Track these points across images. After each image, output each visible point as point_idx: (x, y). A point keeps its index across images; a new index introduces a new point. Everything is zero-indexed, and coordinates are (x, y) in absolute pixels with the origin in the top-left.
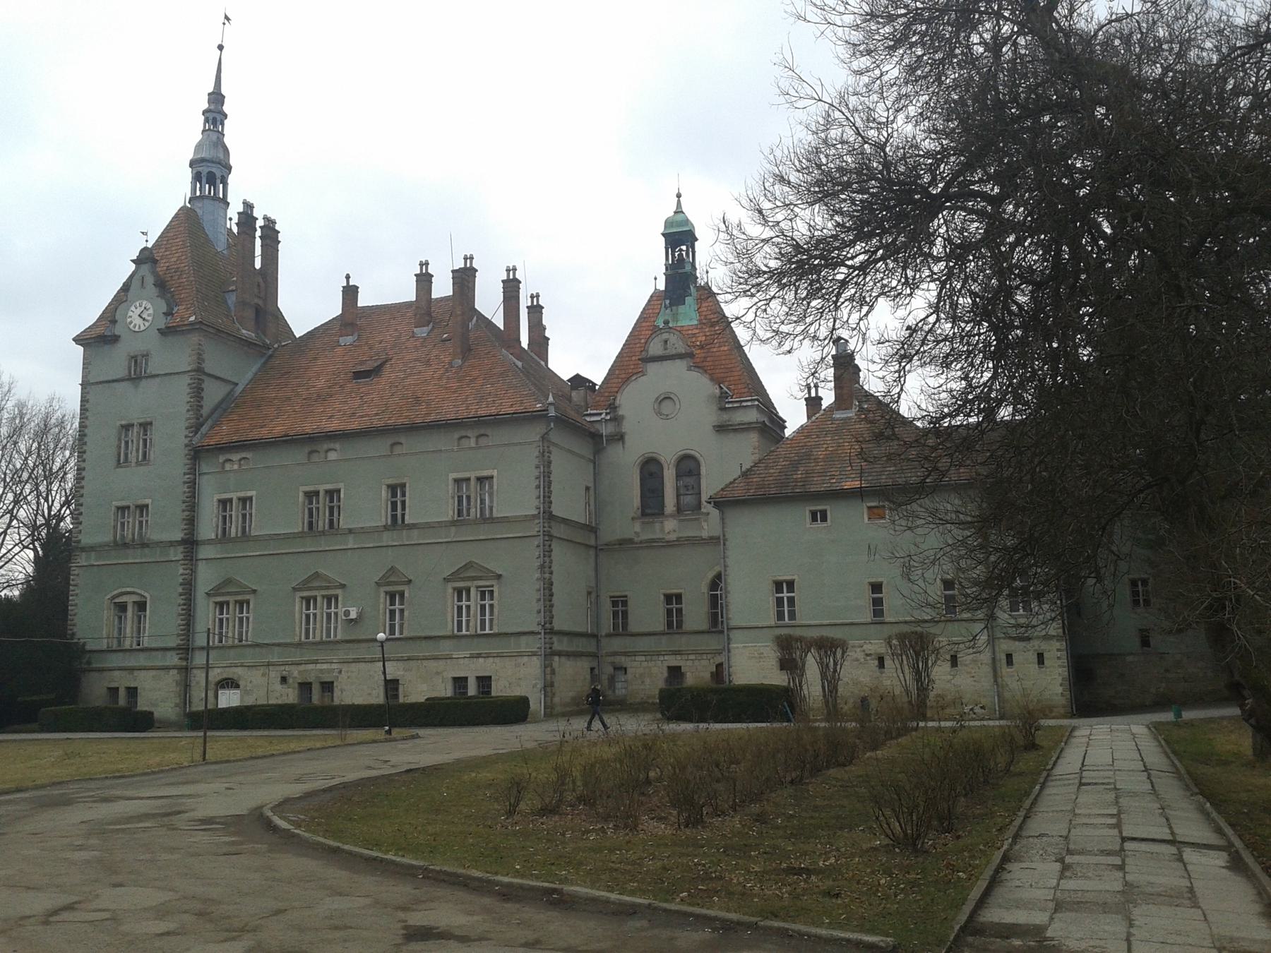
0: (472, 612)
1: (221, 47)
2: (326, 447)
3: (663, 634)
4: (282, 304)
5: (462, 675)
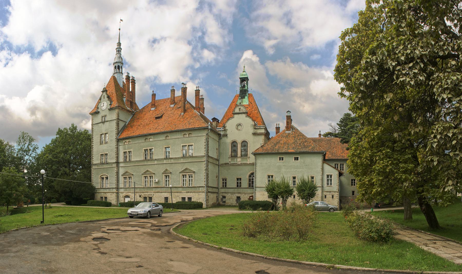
0: (187, 181)
2: (149, 137)
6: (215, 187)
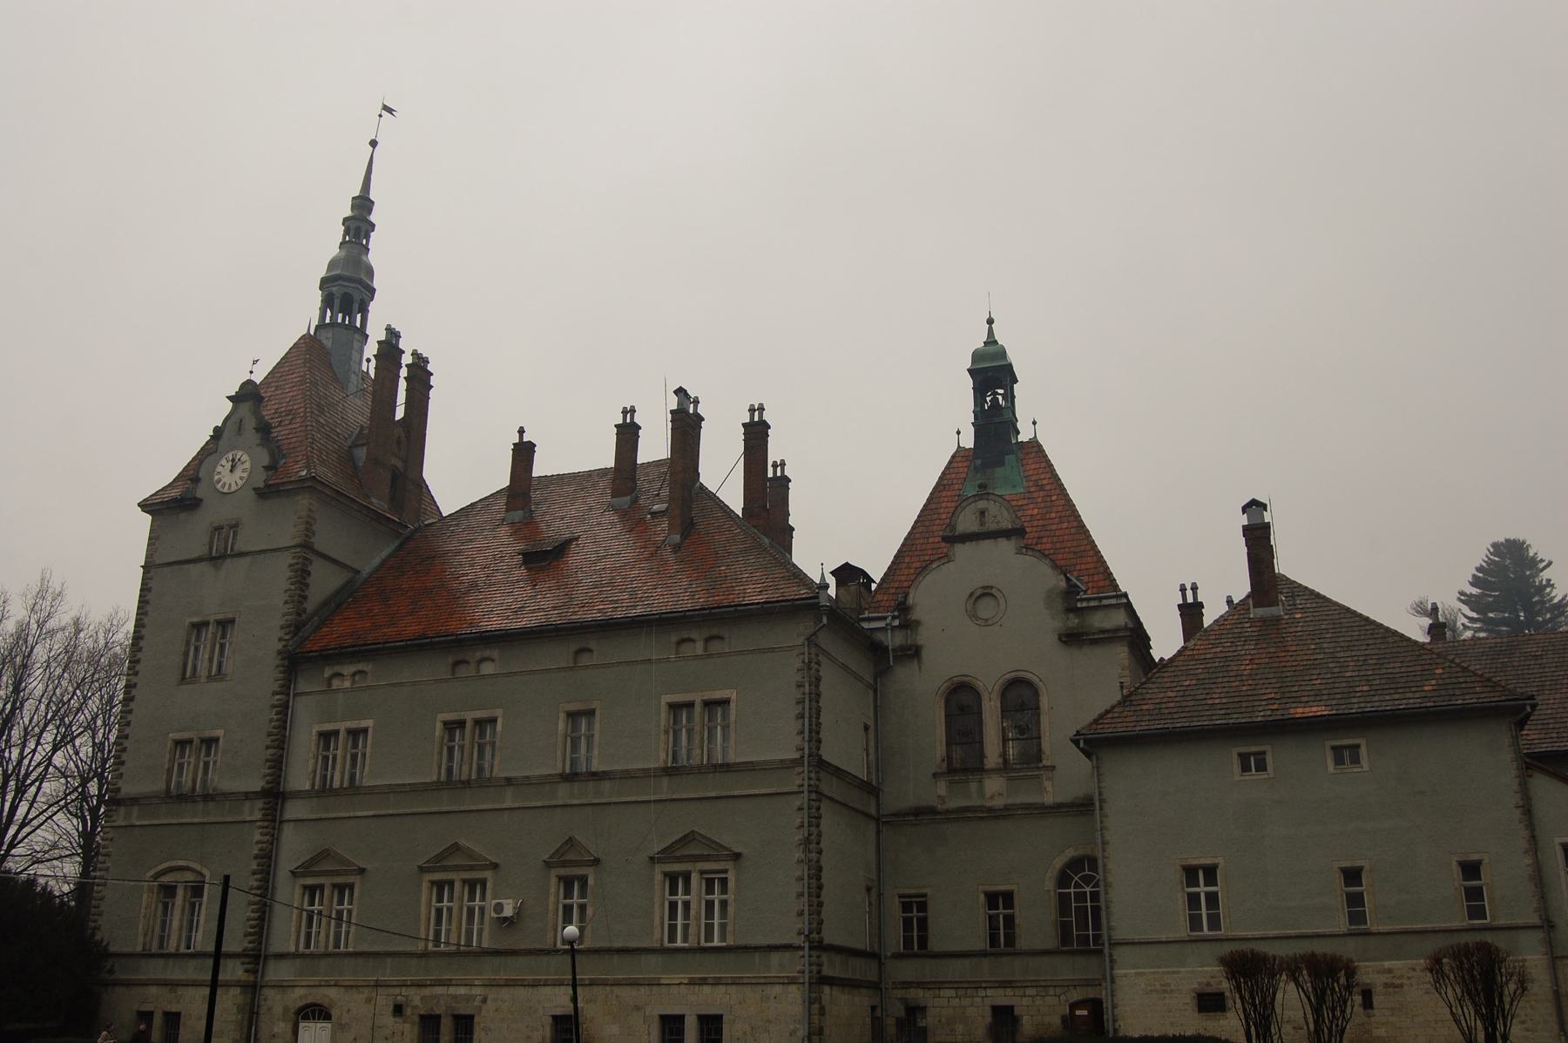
0: (692, 912)
1: (374, 144)
2: (478, 655)
3: (983, 954)
4: (428, 474)
5: (676, 1011)
6: (859, 946)
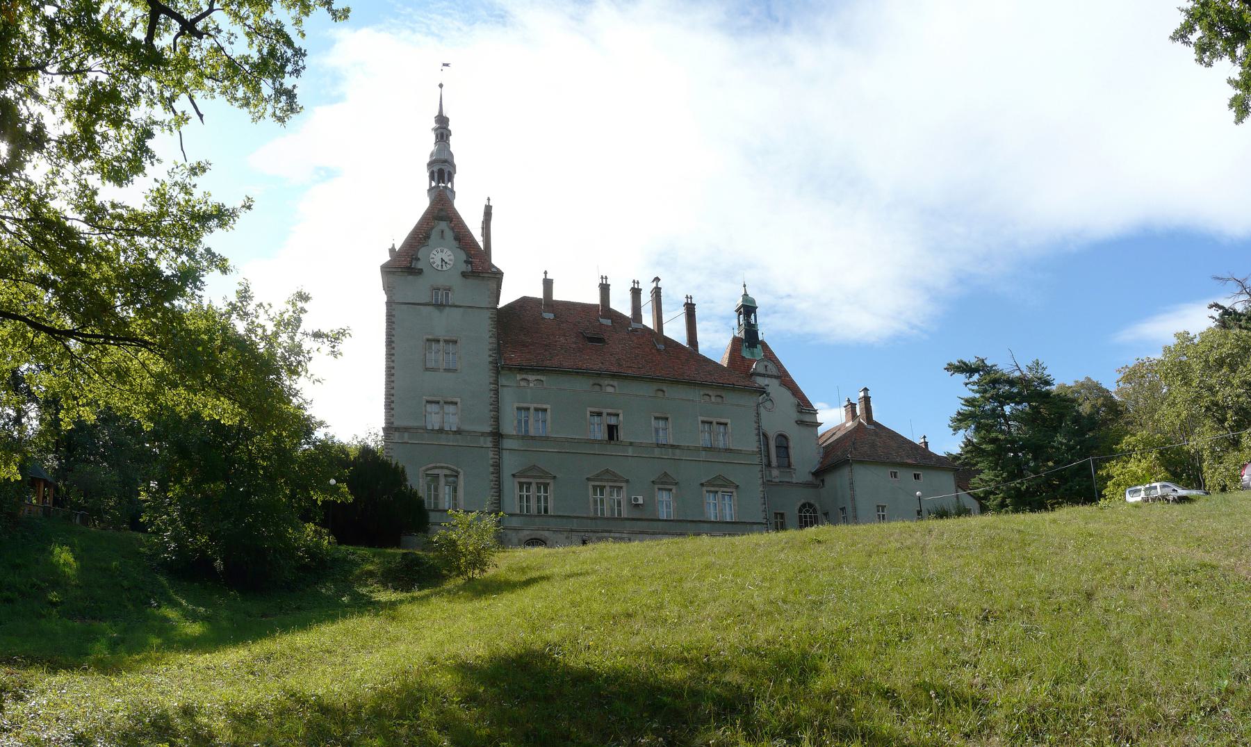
2: (606, 382)
